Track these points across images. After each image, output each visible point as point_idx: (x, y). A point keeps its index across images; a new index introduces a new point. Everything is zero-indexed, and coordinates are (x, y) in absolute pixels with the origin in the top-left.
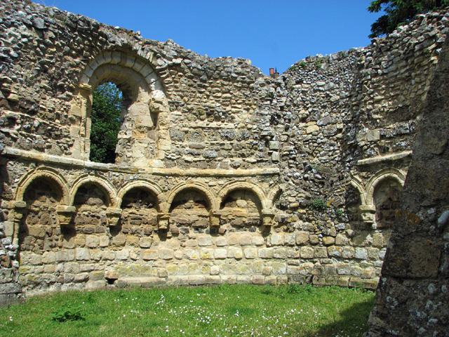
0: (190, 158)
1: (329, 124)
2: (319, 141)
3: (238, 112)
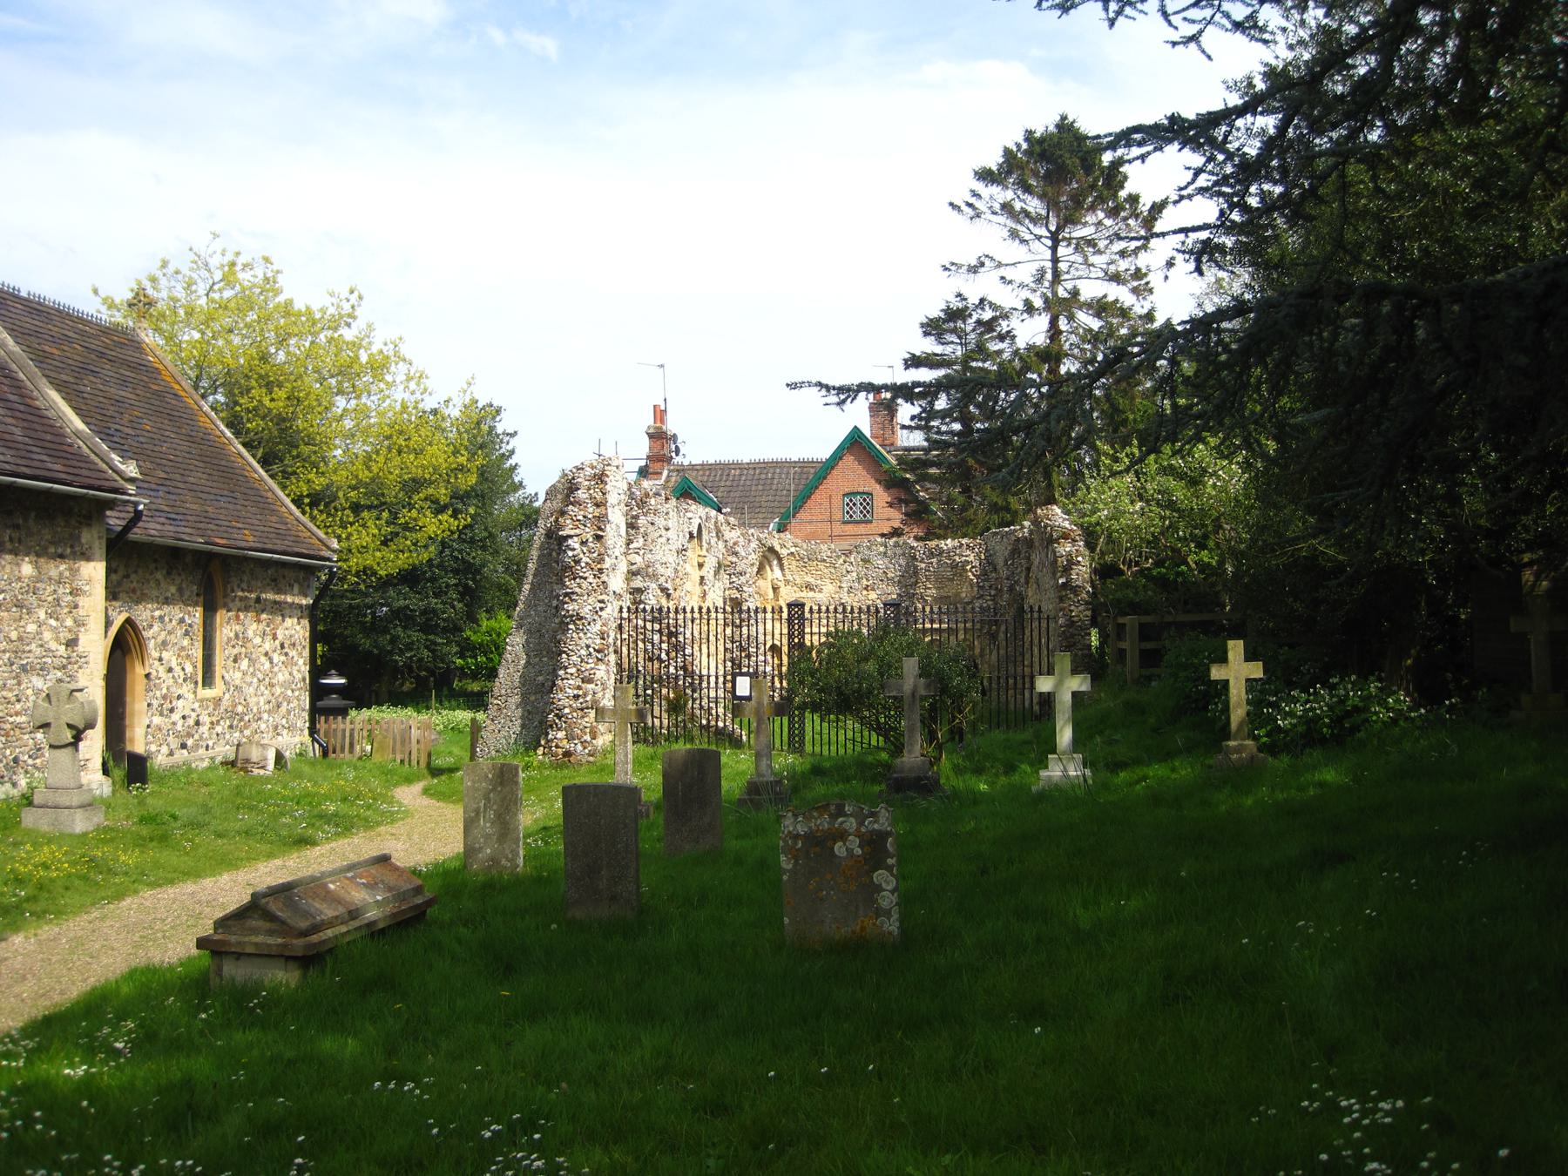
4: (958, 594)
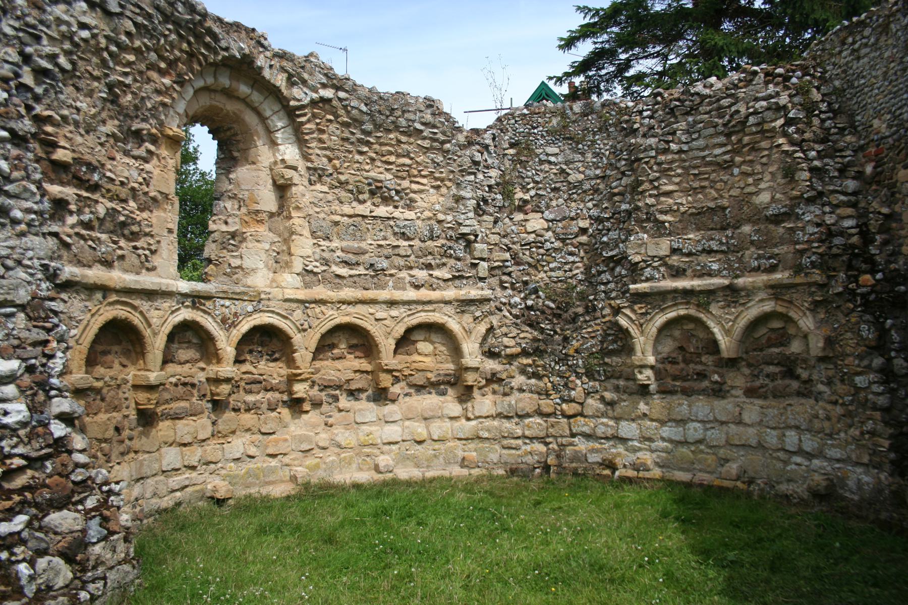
0: (343, 271)
1: (564, 218)
2: (548, 245)
3: (421, 192)
4: (745, 199)
